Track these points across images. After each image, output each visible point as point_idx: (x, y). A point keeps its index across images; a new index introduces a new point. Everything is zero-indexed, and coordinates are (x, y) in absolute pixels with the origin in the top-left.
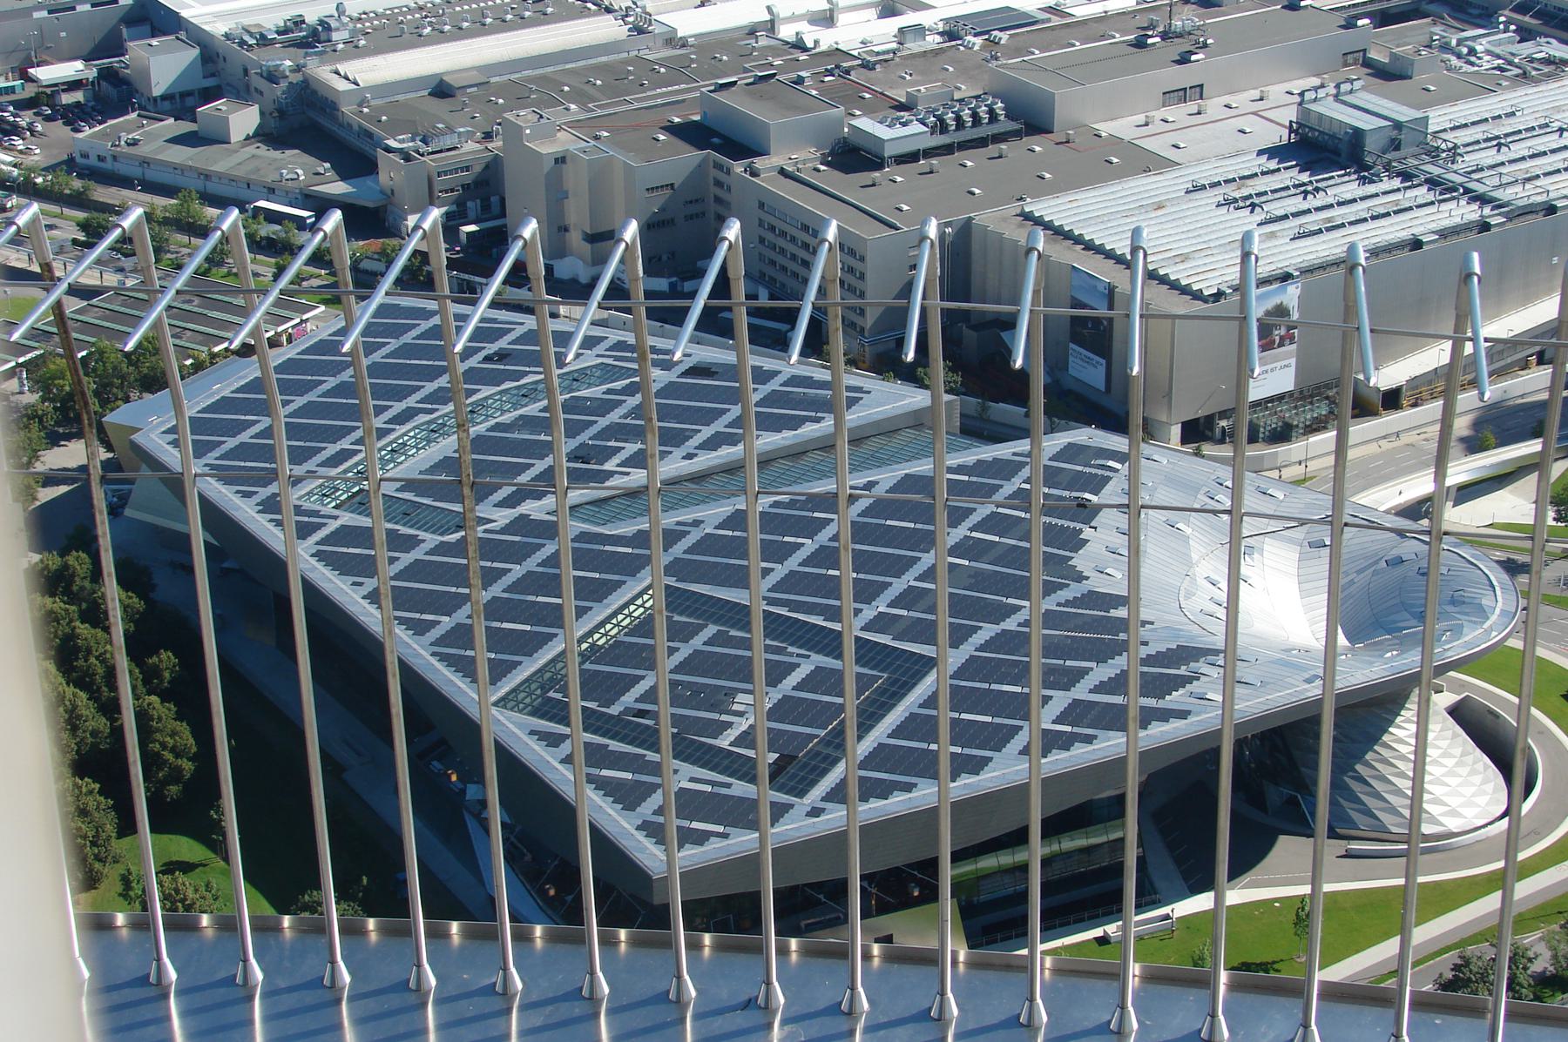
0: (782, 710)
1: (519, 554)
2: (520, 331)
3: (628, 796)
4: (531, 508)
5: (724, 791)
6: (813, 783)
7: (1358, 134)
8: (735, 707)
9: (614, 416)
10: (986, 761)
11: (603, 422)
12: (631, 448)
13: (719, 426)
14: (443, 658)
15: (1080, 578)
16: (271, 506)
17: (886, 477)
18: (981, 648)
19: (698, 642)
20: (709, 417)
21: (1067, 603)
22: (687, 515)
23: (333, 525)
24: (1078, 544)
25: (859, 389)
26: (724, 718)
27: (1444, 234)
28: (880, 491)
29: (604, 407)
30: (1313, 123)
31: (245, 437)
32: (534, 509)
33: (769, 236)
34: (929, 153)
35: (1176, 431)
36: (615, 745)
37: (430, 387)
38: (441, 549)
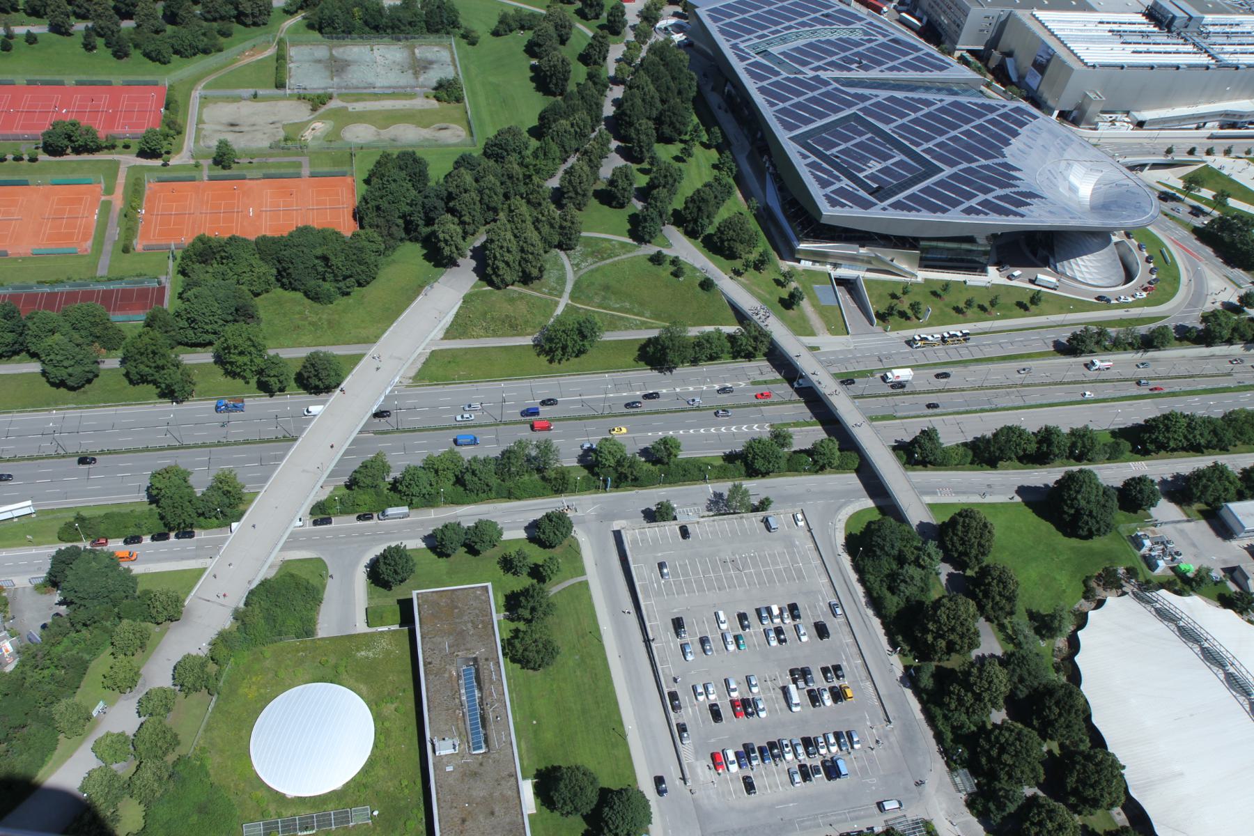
0: (885, 171)
1: (813, 88)
2: (837, 8)
3: (824, 184)
4: (821, 74)
6: (887, 199)
7: (1174, 18)
9: (860, 49)
10: (948, 210)
11: (856, 50)
13: (895, 63)
14: (777, 117)
15: (1004, 156)
16: (734, 47)
17: (949, 99)
19: (864, 138)
20: (893, 59)
23: (753, 60)
24: (1007, 143)
27: (1190, 66)
28: (944, 103)
30: (1157, 8)
31: (733, 20)
32: (821, 74)
35: (1056, 113)
36: (825, 165)
37: (800, 20)
38: (785, 79)
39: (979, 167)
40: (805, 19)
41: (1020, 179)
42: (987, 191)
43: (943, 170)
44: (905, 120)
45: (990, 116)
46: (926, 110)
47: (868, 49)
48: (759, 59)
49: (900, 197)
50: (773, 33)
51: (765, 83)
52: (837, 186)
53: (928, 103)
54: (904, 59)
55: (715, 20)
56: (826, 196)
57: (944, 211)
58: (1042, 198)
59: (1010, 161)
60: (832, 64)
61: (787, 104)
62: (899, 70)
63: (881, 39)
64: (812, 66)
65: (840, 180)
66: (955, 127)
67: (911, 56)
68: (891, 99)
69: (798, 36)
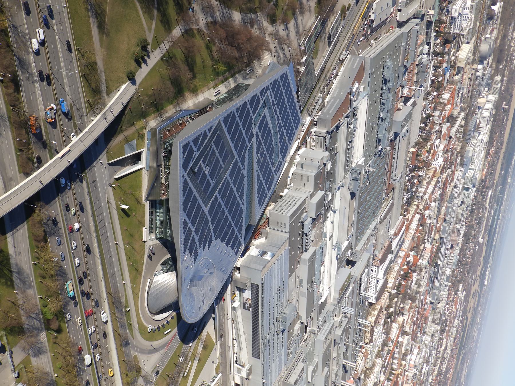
3: (195, 141)
5: (192, 160)
8: (207, 166)
9: (268, 159)
10: (185, 212)
11: (268, 156)
12: (261, 161)
13: (262, 178)
14: (231, 113)
15: (215, 239)
16: (267, 88)
17: (244, 207)
18: (207, 217)
21: (211, 236)
22: (245, 167)
24: (222, 240)
25: (262, 207)
26: (206, 164)
28: (242, 205)
29: (270, 157)
31: (282, 87)
32: (254, 138)
33: (294, 198)
34: (303, 232)
36: (206, 141)
37: (282, 125)
38: (251, 118)
39: (209, 227)
40: (283, 128)
41: (204, 249)
42: (196, 231)
43: (206, 206)
44: (232, 185)
45: (236, 230)
46: (237, 196)
47: (268, 163)
48: (262, 102)
49: (191, 185)
50: (275, 110)
51: (249, 106)
52: (195, 149)
53: (241, 197)
54: (263, 182)
55: (282, 77)
56: (189, 143)
57: (184, 210)
58: (195, 262)
59: (214, 243)
60: (260, 143)
61: (238, 119)
62: (258, 180)
63: (273, 169)
64: (258, 132)
65: (198, 151)
66: (230, 212)
67: (265, 186)
68: (243, 177)
69: (274, 125)
